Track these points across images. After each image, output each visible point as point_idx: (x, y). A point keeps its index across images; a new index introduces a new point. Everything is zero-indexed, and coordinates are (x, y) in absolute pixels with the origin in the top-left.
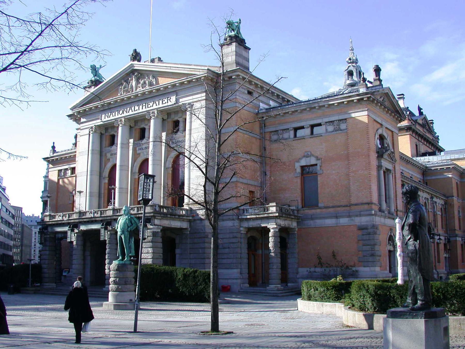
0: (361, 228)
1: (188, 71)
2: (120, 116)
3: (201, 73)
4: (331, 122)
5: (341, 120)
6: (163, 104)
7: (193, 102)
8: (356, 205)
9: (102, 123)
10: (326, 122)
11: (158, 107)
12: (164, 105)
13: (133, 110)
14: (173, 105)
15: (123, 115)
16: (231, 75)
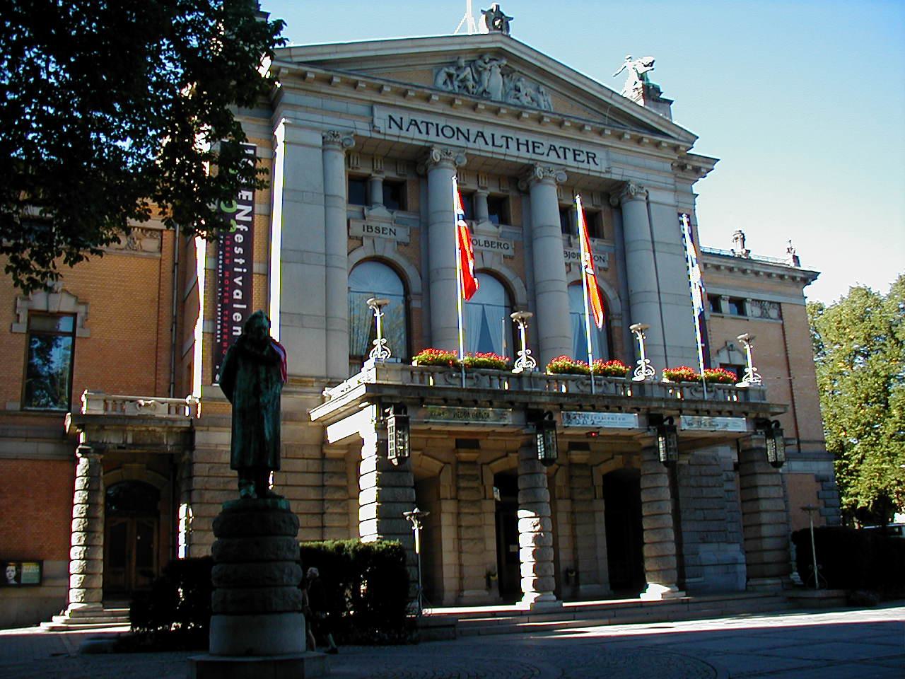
0: (821, 480)
1: (652, 120)
2: (441, 139)
3: (680, 138)
4: (758, 301)
5: (771, 303)
6: (575, 159)
7: (649, 186)
8: (808, 442)
9: (375, 135)
10: (753, 300)
11: (562, 161)
12: (581, 165)
13: (490, 142)
14: (600, 172)
15: (454, 141)
16: (701, 165)
